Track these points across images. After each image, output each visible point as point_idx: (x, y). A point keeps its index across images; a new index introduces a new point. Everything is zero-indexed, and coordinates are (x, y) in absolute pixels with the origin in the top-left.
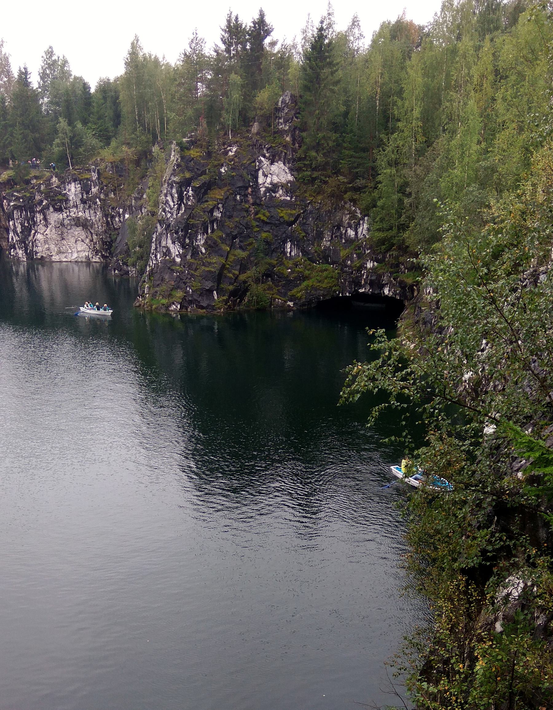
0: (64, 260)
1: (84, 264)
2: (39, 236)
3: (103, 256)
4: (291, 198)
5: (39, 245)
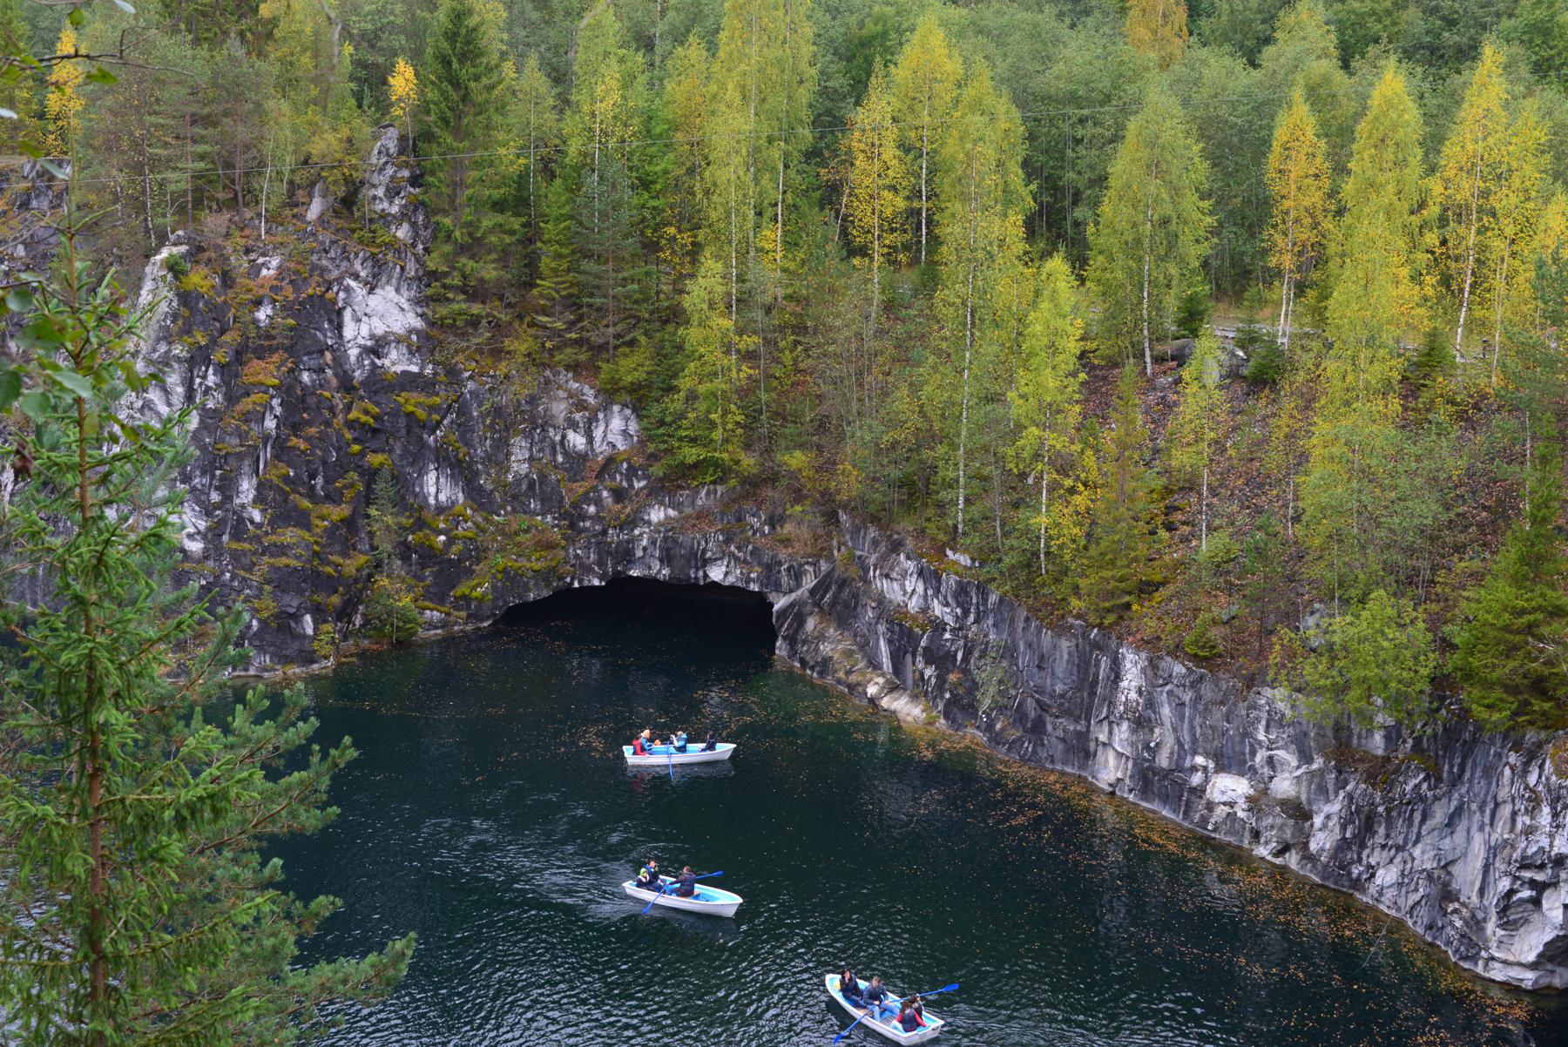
4: (422, 368)
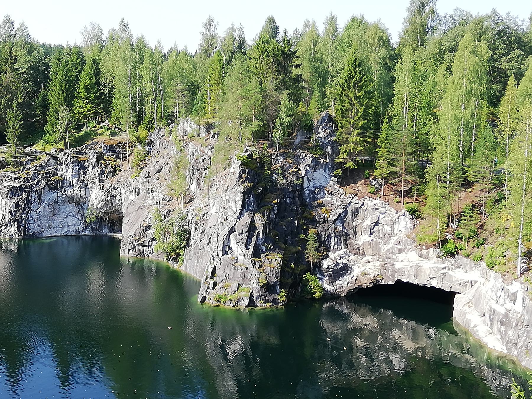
0: (54, 235)
1: (74, 237)
2: (33, 214)
3: (92, 229)
5: (32, 221)
